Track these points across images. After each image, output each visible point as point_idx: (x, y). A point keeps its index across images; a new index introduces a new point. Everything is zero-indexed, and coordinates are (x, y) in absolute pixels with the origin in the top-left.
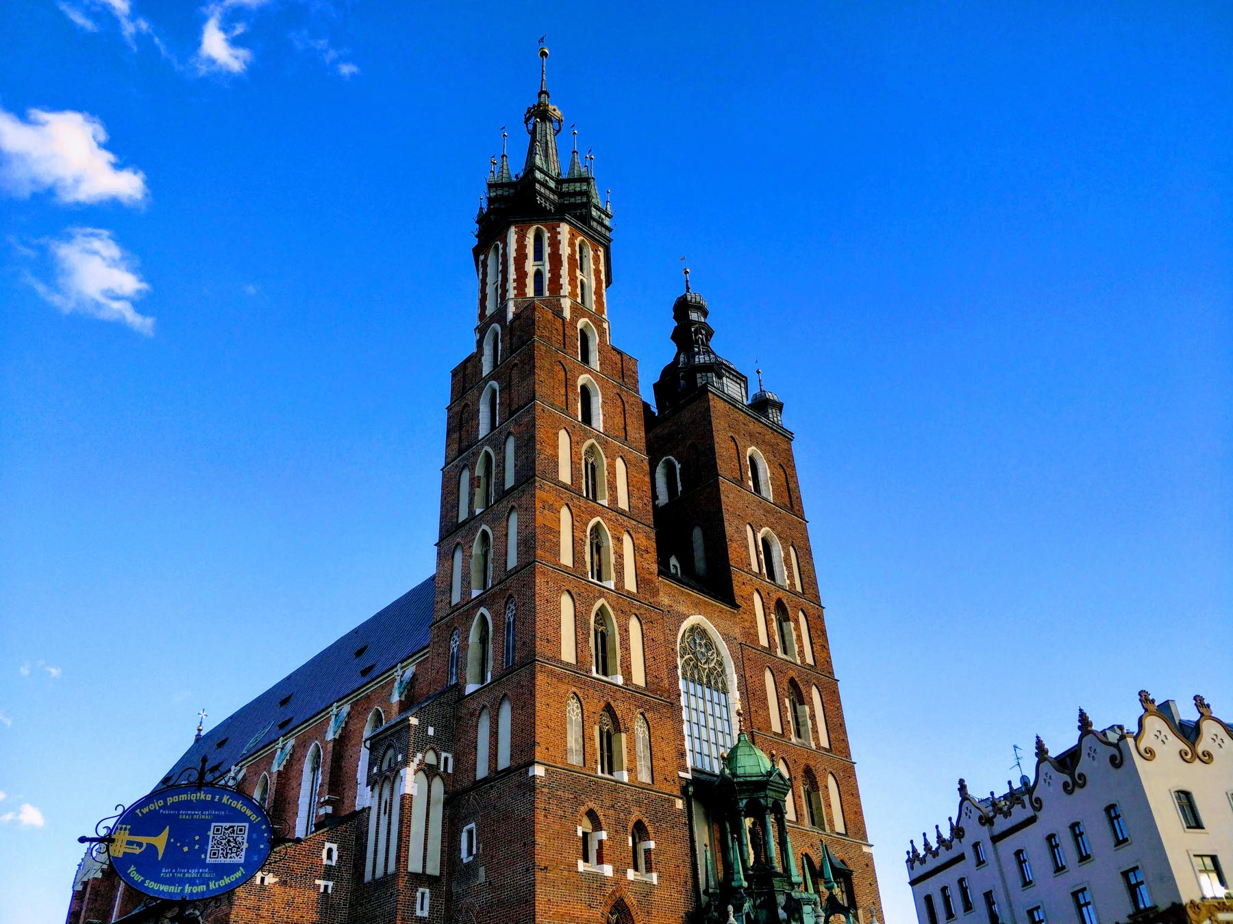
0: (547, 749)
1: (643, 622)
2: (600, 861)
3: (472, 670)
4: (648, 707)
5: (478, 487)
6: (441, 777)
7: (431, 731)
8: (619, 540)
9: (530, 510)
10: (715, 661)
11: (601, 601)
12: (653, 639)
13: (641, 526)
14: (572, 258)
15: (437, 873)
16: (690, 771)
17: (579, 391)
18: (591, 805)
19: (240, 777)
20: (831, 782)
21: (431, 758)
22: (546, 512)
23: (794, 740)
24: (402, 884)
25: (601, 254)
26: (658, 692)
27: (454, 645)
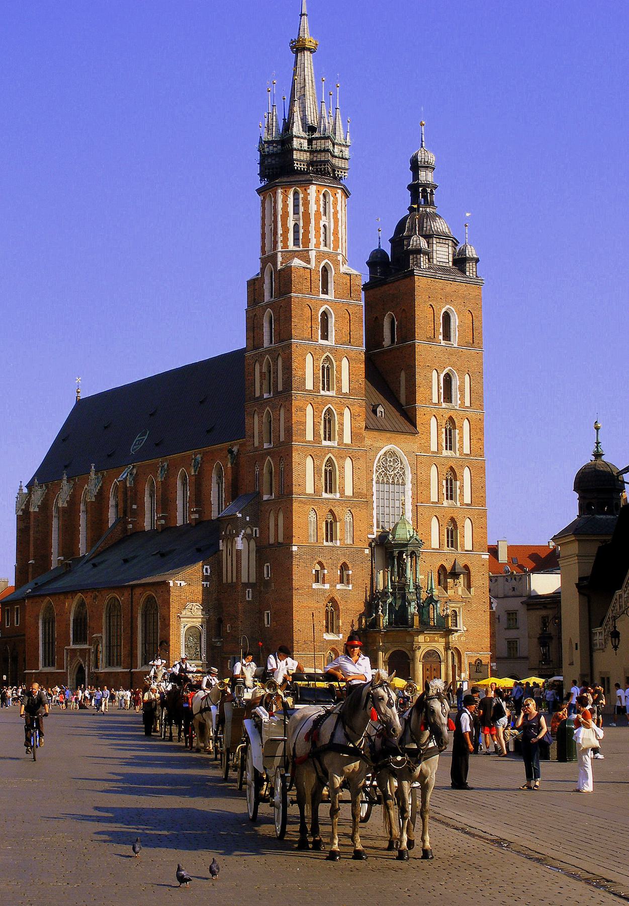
1: (353, 460)
2: (324, 583)
3: (265, 487)
5: (265, 379)
6: (254, 539)
7: (248, 518)
8: (342, 414)
9: (289, 411)
10: (399, 468)
11: (330, 455)
14: (318, 211)
15: (254, 581)
16: (375, 533)
17: (320, 321)
18: (320, 559)
19: (135, 471)
20: (468, 522)
21: (249, 531)
22: (298, 412)
23: (446, 503)
24: (240, 588)
27: (257, 470)
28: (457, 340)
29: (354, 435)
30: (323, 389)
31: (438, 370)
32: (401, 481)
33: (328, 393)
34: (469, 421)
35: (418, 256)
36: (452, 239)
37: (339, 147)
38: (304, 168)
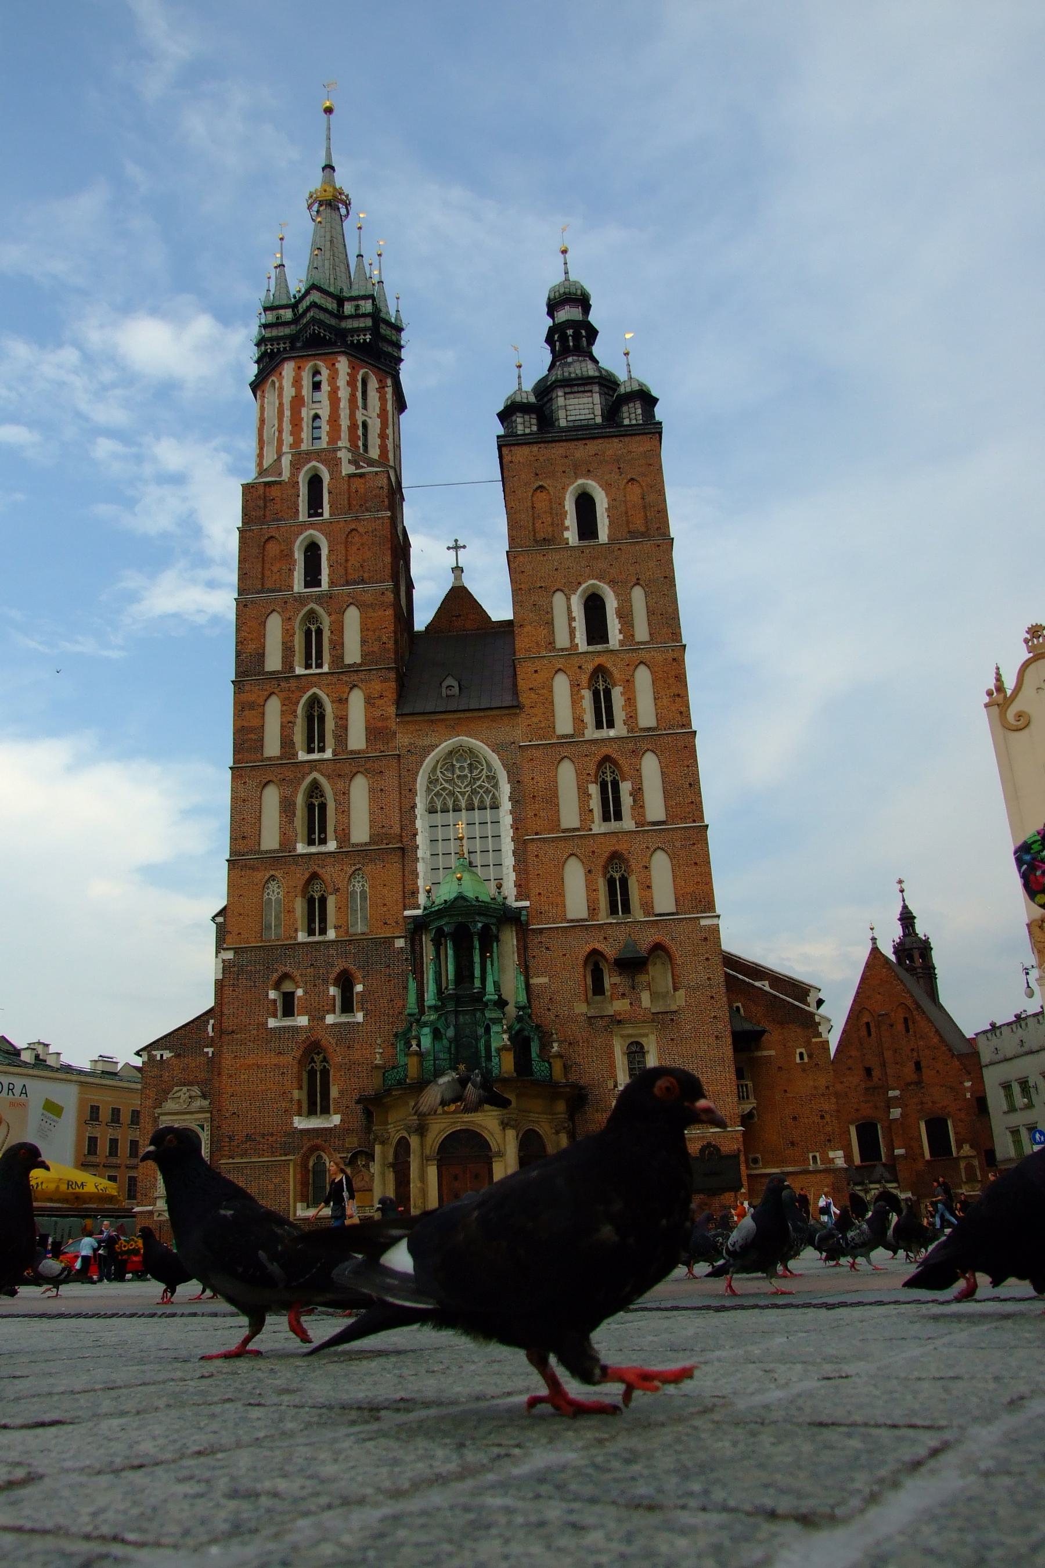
0: (239, 934)
2: (298, 1015)
4: (367, 861)
8: (342, 702)
11: (315, 775)
12: (382, 790)
13: (375, 672)
18: (288, 969)
22: (246, 713)
25: (343, 365)
26: (385, 842)
28: (607, 531)
29: (370, 733)
30: (308, 666)
31: (566, 590)
32: (488, 802)
33: (314, 671)
34: (648, 667)
35: (514, 418)
36: (596, 381)
37: (353, 303)
38: (285, 348)
